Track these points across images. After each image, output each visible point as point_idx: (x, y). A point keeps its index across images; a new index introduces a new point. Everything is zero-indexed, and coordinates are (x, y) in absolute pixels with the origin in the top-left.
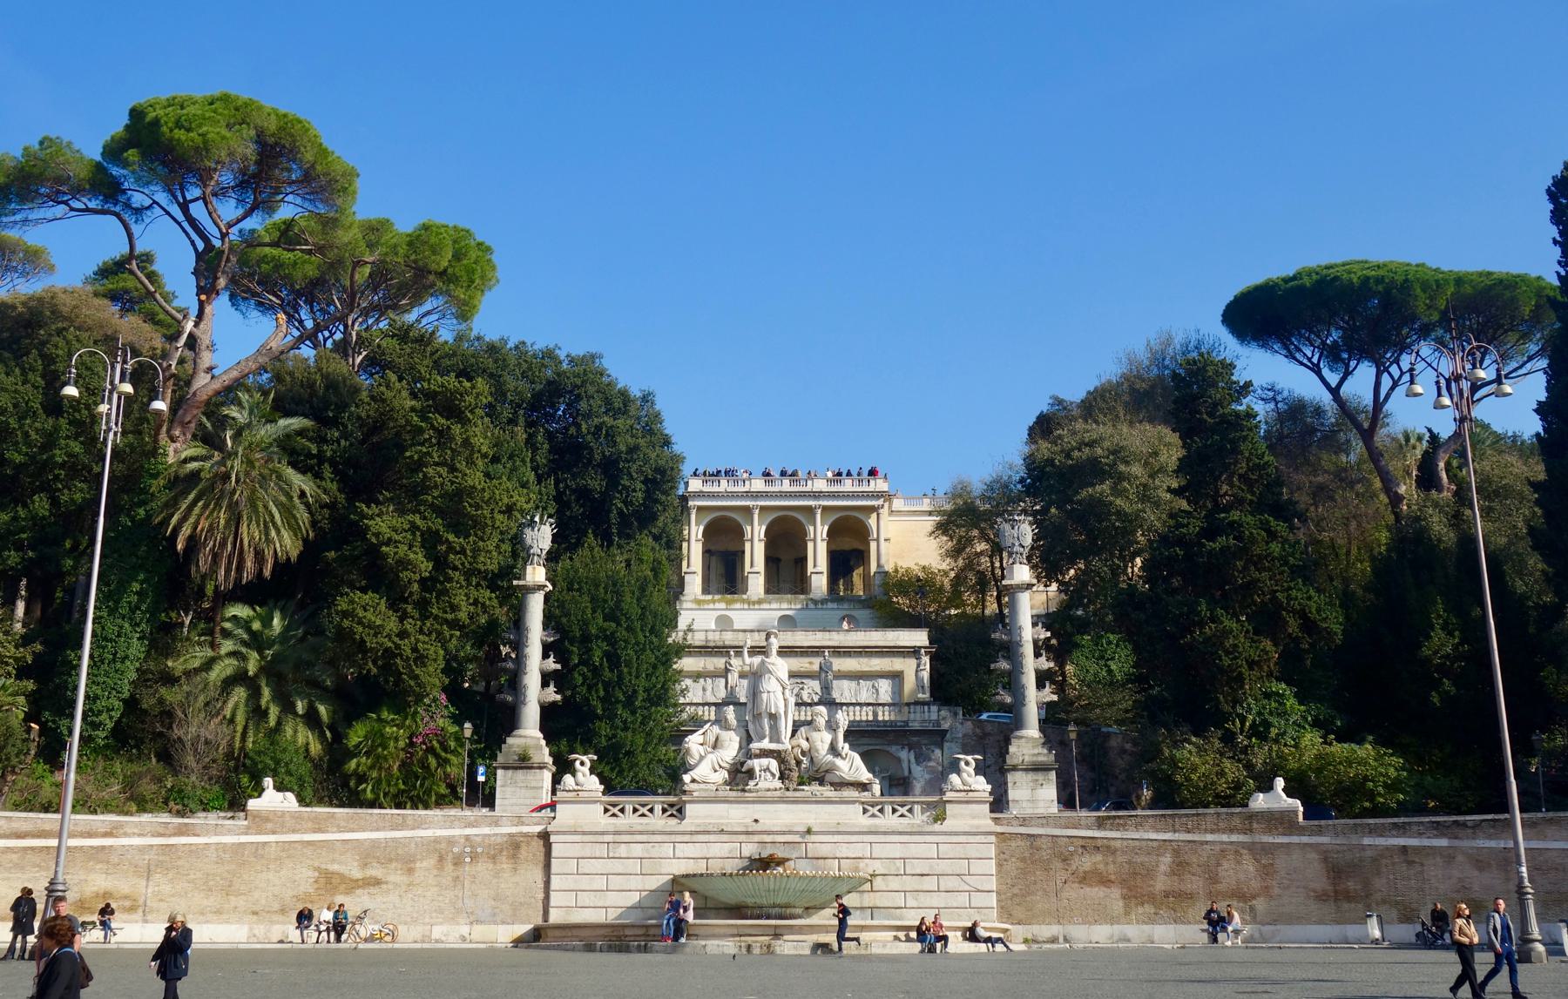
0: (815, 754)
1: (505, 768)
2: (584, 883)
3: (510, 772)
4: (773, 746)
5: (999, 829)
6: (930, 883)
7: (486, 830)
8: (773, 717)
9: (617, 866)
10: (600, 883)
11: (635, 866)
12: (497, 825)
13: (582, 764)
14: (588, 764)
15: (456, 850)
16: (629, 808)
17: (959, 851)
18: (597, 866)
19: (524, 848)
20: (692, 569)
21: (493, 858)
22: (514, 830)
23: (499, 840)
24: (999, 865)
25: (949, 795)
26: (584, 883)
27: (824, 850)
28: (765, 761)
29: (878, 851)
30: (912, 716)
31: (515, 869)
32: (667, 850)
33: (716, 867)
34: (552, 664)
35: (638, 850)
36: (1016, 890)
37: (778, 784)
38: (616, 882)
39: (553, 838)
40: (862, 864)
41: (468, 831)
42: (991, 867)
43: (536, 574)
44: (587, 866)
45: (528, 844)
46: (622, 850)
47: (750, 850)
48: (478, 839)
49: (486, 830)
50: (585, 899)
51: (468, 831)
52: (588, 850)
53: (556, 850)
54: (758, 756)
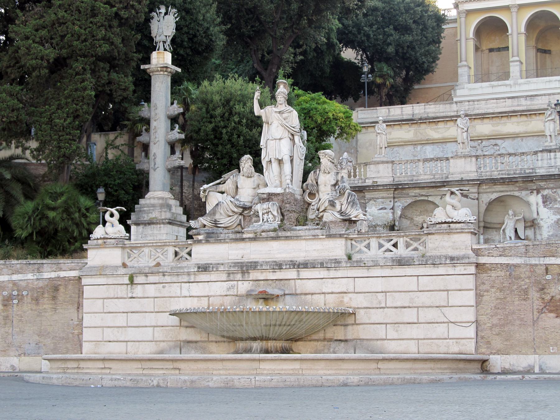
1: (137, 224)
2: (109, 320)
3: (141, 228)
5: (482, 260)
6: (409, 315)
7: (30, 276)
8: (280, 162)
9: (135, 305)
10: (121, 320)
11: (148, 305)
12: (39, 271)
13: (112, 215)
15: (5, 293)
17: (439, 283)
18: (121, 305)
19: (62, 289)
21: (36, 300)
22: (53, 275)
23: (41, 284)
24: (479, 296)
26: (109, 320)
27: (310, 286)
29: (361, 285)
30: (540, 164)
31: (55, 309)
32: (175, 289)
33: (216, 304)
34: (177, 134)
35: (151, 290)
36: (495, 321)
38: (135, 319)
39: (84, 281)
40: (346, 298)
41: (15, 277)
42: (470, 298)
43: (162, 59)
44: (112, 305)
45: (66, 286)
46: (138, 291)
47: (244, 287)
48: (23, 284)
49: (30, 276)
50: (109, 334)
51: (15, 277)
52: (112, 291)
53: (88, 292)
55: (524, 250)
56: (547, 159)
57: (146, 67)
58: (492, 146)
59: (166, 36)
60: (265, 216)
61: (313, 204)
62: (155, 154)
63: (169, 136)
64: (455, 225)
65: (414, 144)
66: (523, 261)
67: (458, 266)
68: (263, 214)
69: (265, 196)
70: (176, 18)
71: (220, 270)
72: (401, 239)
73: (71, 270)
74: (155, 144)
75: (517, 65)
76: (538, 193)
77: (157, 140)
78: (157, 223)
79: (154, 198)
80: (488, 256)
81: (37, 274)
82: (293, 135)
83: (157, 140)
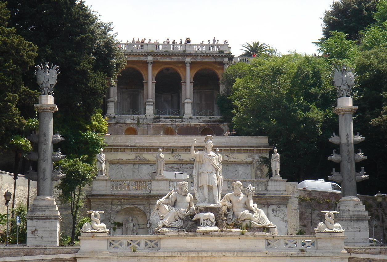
0: (235, 210)
4: (212, 205)
12: (44, 254)
14: (99, 216)
16: (125, 242)
20: (112, 99)
25: (318, 235)
28: (207, 214)
37: (215, 228)
54: (201, 211)
55: (379, 251)
56: (274, 185)
57: (38, 105)
58: (189, 169)
59: (51, 85)
60: (205, 222)
61: (229, 215)
62: (44, 169)
63: (54, 157)
64: (334, 233)
65: (134, 163)
66: (378, 257)
67: (337, 259)
68: (204, 220)
69: (203, 209)
70: (57, 72)
71: (183, 255)
72: (300, 241)
73: (67, 253)
74: (44, 161)
75: (151, 105)
76: (268, 207)
77: (46, 158)
78: (49, 219)
79: (44, 200)
80: (355, 253)
81: (43, 256)
82: (216, 171)
83: (46, 158)
